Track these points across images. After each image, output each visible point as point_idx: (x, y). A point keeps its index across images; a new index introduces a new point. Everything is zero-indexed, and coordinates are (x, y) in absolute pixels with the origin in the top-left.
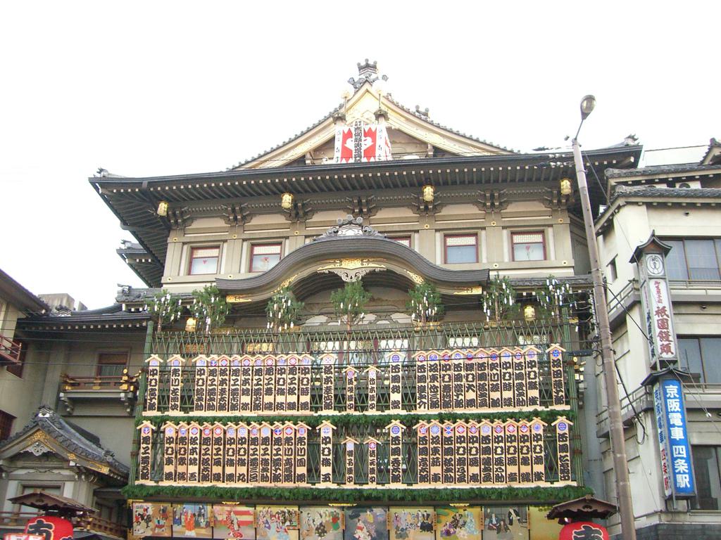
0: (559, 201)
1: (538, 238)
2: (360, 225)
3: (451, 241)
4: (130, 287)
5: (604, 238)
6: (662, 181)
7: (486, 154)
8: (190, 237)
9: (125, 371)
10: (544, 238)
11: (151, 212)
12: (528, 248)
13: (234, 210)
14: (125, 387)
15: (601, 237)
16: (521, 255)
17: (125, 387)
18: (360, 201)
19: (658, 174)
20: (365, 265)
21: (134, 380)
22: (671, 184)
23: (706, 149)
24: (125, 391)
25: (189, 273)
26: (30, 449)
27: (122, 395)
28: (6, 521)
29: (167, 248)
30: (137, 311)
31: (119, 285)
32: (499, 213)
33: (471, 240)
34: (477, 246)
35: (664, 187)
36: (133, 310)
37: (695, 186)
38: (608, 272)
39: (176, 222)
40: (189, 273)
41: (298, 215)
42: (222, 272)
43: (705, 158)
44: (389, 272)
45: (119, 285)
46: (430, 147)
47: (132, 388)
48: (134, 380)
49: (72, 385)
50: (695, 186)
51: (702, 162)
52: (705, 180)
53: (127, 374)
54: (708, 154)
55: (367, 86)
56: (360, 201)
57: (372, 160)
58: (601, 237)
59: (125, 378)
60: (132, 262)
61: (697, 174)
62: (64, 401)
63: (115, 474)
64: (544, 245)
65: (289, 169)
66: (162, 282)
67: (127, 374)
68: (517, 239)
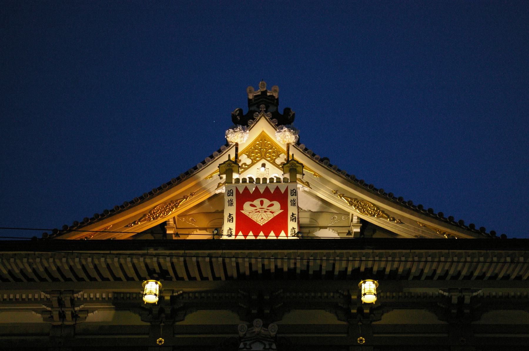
57: (282, 236)
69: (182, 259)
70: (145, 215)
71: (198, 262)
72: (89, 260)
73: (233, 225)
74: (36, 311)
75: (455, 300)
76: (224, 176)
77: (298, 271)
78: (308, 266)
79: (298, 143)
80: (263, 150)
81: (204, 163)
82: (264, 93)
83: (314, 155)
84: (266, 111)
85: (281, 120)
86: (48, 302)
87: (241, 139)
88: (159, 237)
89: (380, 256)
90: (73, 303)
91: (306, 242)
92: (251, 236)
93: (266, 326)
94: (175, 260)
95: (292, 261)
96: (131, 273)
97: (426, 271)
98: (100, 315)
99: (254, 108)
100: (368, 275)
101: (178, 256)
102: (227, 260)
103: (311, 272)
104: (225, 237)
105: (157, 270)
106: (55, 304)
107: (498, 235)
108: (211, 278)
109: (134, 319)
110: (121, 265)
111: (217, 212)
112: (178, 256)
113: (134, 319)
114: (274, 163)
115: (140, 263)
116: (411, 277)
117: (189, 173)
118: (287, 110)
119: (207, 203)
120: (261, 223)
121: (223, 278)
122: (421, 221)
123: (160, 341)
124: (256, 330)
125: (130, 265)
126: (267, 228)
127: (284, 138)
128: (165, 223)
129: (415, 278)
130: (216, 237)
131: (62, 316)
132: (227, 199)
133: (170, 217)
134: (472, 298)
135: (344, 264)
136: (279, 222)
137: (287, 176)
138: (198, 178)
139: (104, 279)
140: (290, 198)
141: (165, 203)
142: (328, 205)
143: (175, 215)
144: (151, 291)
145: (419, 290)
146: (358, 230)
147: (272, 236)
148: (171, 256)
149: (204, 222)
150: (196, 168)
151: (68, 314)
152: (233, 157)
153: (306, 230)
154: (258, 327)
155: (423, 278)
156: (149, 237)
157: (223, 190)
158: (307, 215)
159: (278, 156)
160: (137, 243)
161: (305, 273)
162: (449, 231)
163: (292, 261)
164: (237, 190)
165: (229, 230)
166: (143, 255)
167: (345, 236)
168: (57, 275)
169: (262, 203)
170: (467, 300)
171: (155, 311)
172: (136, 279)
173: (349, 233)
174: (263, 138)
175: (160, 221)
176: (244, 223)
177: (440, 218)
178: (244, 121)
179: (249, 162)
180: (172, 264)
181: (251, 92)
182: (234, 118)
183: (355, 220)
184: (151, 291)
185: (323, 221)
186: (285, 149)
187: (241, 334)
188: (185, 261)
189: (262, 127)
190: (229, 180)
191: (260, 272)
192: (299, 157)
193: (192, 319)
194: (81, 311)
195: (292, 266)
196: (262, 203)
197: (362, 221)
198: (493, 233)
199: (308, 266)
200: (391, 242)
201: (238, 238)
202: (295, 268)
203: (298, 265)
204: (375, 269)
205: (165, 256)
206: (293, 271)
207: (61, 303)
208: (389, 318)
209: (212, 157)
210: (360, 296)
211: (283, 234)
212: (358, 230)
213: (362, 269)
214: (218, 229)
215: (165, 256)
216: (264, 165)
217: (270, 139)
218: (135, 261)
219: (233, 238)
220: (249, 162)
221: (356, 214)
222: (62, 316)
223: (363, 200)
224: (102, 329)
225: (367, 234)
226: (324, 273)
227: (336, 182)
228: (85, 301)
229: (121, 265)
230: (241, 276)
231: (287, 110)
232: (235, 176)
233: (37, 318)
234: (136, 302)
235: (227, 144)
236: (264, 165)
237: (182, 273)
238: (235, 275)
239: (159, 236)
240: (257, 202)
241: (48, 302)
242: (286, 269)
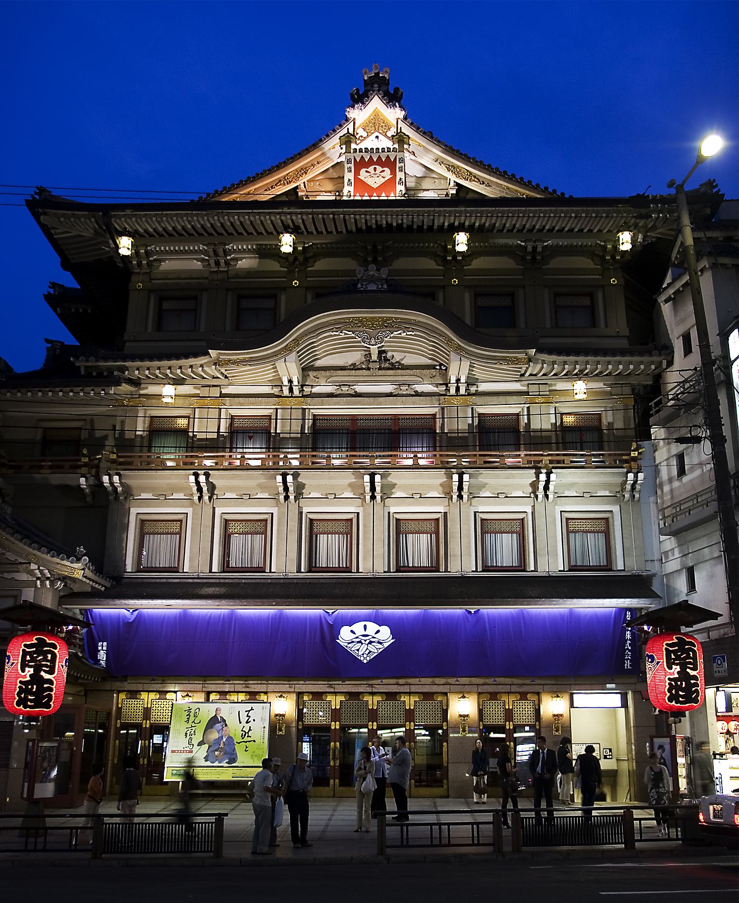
5: (675, 306)
18: (375, 247)
38: (678, 346)
40: (159, 327)
49: (11, 467)
56: (375, 247)
66: (125, 338)
69: (310, 216)
70: (280, 181)
71: (323, 219)
72: (235, 218)
73: (352, 189)
74: (197, 260)
75: (530, 249)
76: (344, 147)
77: (405, 226)
78: (413, 221)
79: (405, 118)
80: (376, 125)
81: (328, 136)
82: (377, 74)
83: (418, 128)
84: (379, 91)
85: (392, 99)
86: (205, 252)
87: (359, 115)
88: (292, 199)
89: (471, 212)
90: (226, 253)
91: (411, 202)
93: (378, 270)
94: (305, 217)
95: (400, 217)
96: (270, 228)
97: (507, 225)
98: (246, 263)
99: (369, 87)
100: (461, 228)
101: (307, 214)
102: (347, 217)
103: (415, 227)
104: (345, 198)
105: (291, 224)
106: (212, 254)
107: (567, 196)
108: (335, 233)
109: (274, 266)
110: (262, 222)
111: (339, 177)
112: (307, 214)
113: (274, 266)
114: (386, 136)
115: (277, 219)
116: (495, 231)
117: (315, 145)
118: (396, 90)
119: (331, 170)
120: (375, 186)
121: (345, 232)
122: (506, 184)
123: (296, 283)
124: (371, 273)
125: (269, 222)
127: (394, 114)
128: (297, 187)
129: (498, 231)
130: (338, 198)
131: (217, 264)
132: (347, 166)
133: (300, 183)
134: (544, 247)
135: (442, 221)
136: (390, 184)
137: (396, 146)
138: (323, 148)
139: (249, 234)
140: (398, 165)
141: (296, 170)
142: (429, 170)
143: (305, 180)
144: (287, 243)
145: (502, 241)
146: (454, 192)
148: (301, 213)
149: (329, 186)
150: (321, 140)
151: (222, 261)
152: (351, 131)
153: (413, 192)
154: (372, 270)
155: (505, 231)
156: (284, 198)
157: (343, 159)
158: (414, 179)
159: (389, 129)
160: (274, 203)
161: (410, 228)
162: (528, 192)
163: (400, 217)
164: (355, 159)
165: (349, 192)
166: (279, 213)
167: (443, 197)
168: (212, 231)
169: (375, 169)
170: (539, 249)
171: (291, 259)
172: (275, 233)
173: (447, 195)
174: (376, 115)
175: (293, 185)
176: (359, 184)
177: (520, 182)
178: (360, 99)
179: (365, 134)
180: (303, 220)
181: (366, 73)
182: (352, 96)
183: (452, 184)
184: (287, 243)
185: (426, 184)
186: (395, 123)
187: (359, 276)
188: (313, 218)
189: (376, 104)
190: (348, 151)
191: (374, 226)
192: (406, 130)
193: (320, 265)
194: (232, 259)
195: (400, 222)
196: (375, 169)
197: (457, 184)
198: (563, 194)
199: (413, 221)
200: (481, 201)
201: (356, 198)
202: (402, 223)
203: (405, 221)
204: (467, 223)
205: (296, 214)
206: (400, 226)
207: (216, 253)
208: (478, 263)
209: (334, 131)
210: (454, 246)
211: (392, 194)
212: (454, 192)
213: (456, 224)
214: (340, 191)
215: (296, 214)
216: (377, 137)
217: (382, 115)
218: (273, 218)
219: (352, 198)
220: (365, 134)
221: (453, 178)
222: (217, 264)
223: (458, 167)
224: (249, 273)
225: (462, 195)
226: (425, 227)
227: (437, 152)
228: (235, 251)
229: (262, 222)
230: (359, 230)
231: (396, 90)
232: (353, 146)
233: (198, 265)
234: (274, 253)
235: (347, 120)
236: (377, 137)
237: (311, 228)
238: (354, 230)
239: (293, 198)
240: (371, 169)
241: (205, 252)
242: (395, 224)
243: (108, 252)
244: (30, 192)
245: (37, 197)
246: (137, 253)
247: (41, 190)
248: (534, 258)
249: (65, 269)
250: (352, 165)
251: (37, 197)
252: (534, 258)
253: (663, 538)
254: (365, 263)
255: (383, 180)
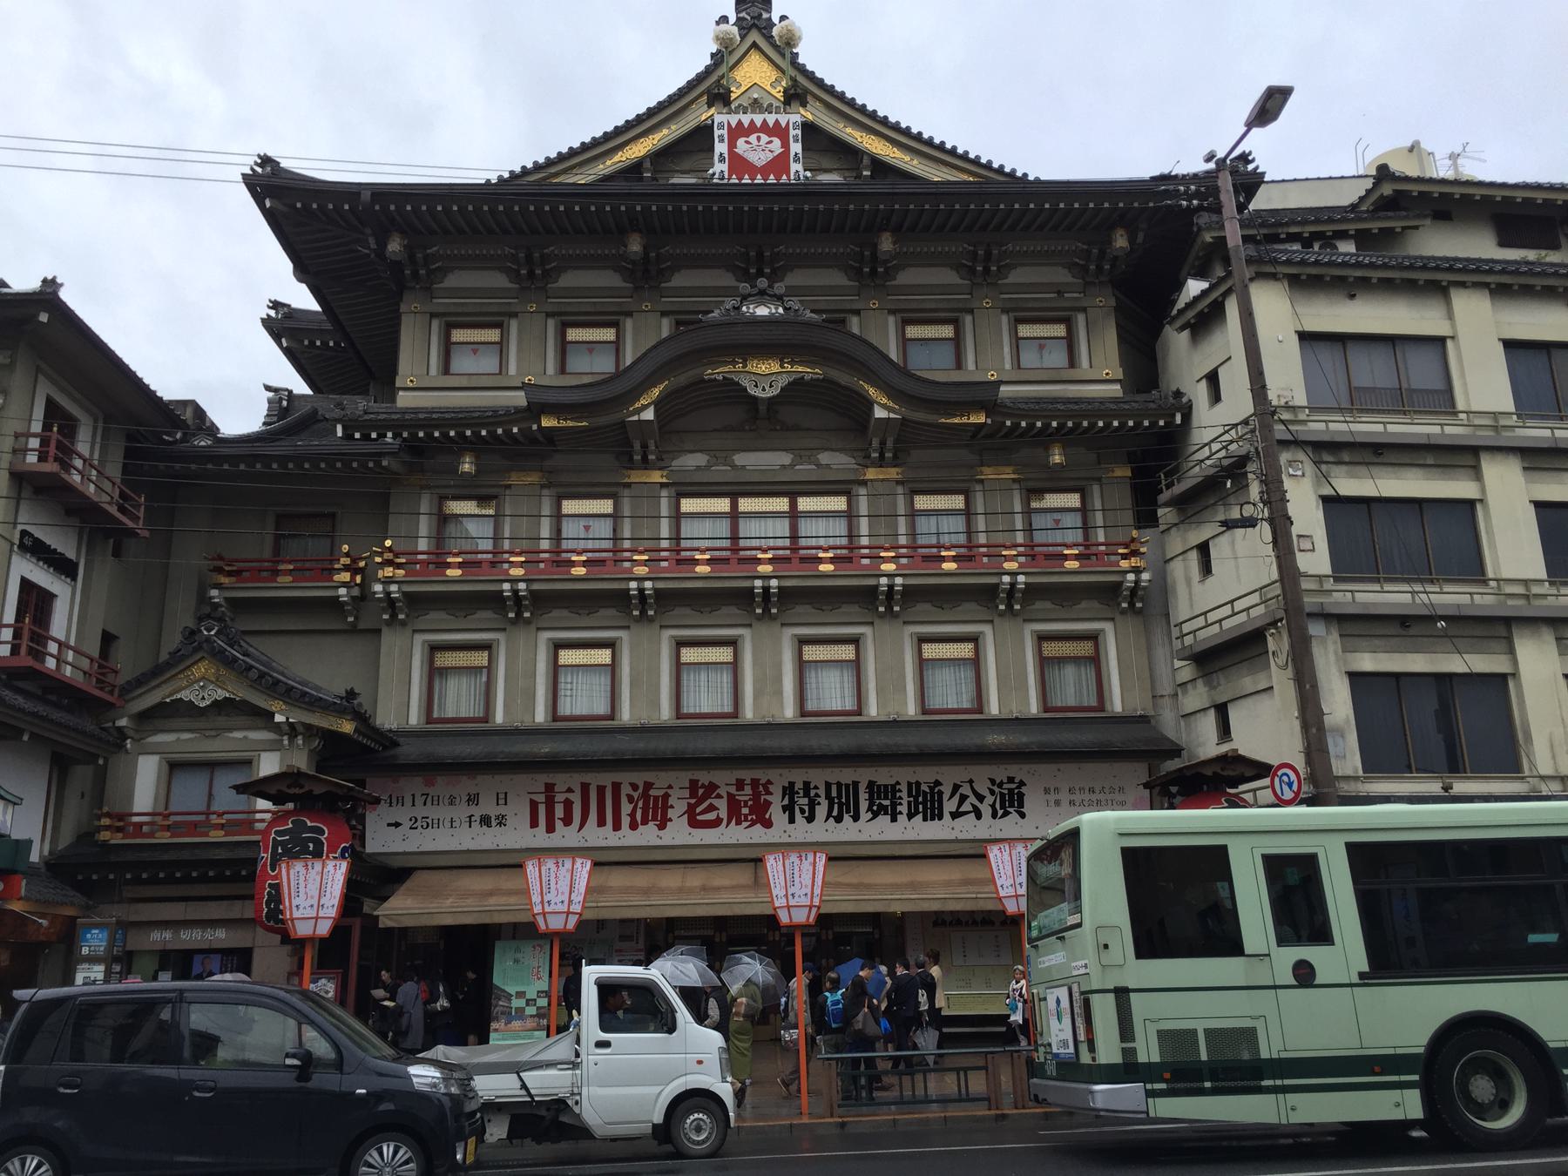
0: (1099, 268)
1: (1059, 330)
2: (779, 298)
3: (913, 332)
4: (290, 392)
6: (1292, 238)
7: (965, 177)
8: (441, 302)
9: (345, 548)
10: (957, 332)
11: (361, 252)
12: (1041, 347)
13: (529, 257)
14: (346, 577)
15: (1186, 334)
16: (1029, 358)
17: (345, 576)
18: (760, 255)
19: (1287, 224)
20: (788, 367)
21: (362, 564)
22: (1307, 244)
23: (1369, 184)
24: (344, 585)
25: (446, 371)
26: (185, 695)
27: (342, 591)
28: (145, 829)
29: (399, 324)
30: (366, 437)
31: (268, 388)
32: (996, 284)
33: (947, 331)
34: (957, 341)
35: (1296, 247)
36: (357, 435)
37: (1347, 247)
39: (415, 274)
40: (446, 371)
41: (646, 276)
42: (512, 370)
43: (1362, 199)
44: (827, 381)
45: (268, 388)
46: (866, 161)
47: (358, 579)
48: (362, 564)
49: (230, 574)
50: (1347, 247)
51: (1354, 207)
52: (1362, 239)
53: (347, 555)
54: (1368, 192)
55: (754, 36)
56: (760, 255)
58: (1186, 334)
59: (345, 561)
60: (294, 345)
61: (1351, 227)
62: (217, 605)
63: (365, 736)
64: (1070, 342)
65: (620, 186)
66: (398, 384)
67: (347, 555)
68: (1025, 330)
73: (725, 167)
92: (747, 180)
107: (1031, 178)
120: (759, 164)
126: (765, 170)
147: (772, 179)
169: (759, 139)
196: (759, 139)
207: (529, 257)
240: (753, 138)
243: (368, 255)
244: (247, 164)
245: (259, 170)
246: (412, 258)
247: (266, 161)
248: (987, 271)
249: (300, 280)
250: (725, 132)
251: (259, 170)
252: (987, 271)
253: (1178, 664)
254: (745, 276)
255: (770, 156)
